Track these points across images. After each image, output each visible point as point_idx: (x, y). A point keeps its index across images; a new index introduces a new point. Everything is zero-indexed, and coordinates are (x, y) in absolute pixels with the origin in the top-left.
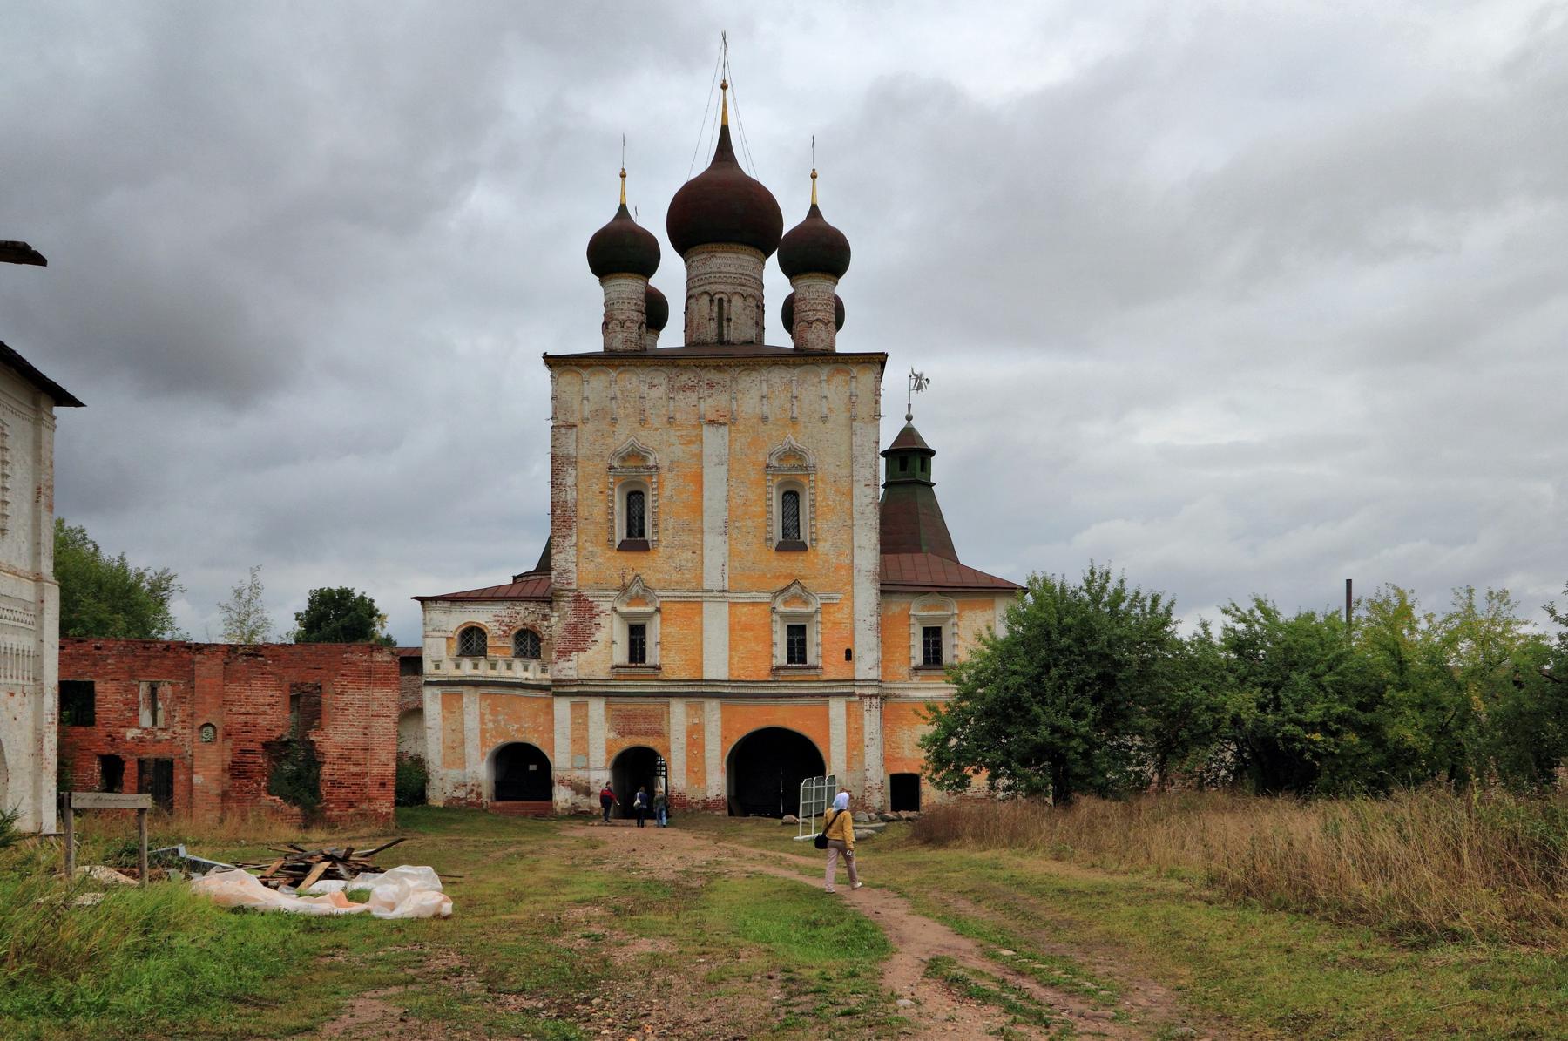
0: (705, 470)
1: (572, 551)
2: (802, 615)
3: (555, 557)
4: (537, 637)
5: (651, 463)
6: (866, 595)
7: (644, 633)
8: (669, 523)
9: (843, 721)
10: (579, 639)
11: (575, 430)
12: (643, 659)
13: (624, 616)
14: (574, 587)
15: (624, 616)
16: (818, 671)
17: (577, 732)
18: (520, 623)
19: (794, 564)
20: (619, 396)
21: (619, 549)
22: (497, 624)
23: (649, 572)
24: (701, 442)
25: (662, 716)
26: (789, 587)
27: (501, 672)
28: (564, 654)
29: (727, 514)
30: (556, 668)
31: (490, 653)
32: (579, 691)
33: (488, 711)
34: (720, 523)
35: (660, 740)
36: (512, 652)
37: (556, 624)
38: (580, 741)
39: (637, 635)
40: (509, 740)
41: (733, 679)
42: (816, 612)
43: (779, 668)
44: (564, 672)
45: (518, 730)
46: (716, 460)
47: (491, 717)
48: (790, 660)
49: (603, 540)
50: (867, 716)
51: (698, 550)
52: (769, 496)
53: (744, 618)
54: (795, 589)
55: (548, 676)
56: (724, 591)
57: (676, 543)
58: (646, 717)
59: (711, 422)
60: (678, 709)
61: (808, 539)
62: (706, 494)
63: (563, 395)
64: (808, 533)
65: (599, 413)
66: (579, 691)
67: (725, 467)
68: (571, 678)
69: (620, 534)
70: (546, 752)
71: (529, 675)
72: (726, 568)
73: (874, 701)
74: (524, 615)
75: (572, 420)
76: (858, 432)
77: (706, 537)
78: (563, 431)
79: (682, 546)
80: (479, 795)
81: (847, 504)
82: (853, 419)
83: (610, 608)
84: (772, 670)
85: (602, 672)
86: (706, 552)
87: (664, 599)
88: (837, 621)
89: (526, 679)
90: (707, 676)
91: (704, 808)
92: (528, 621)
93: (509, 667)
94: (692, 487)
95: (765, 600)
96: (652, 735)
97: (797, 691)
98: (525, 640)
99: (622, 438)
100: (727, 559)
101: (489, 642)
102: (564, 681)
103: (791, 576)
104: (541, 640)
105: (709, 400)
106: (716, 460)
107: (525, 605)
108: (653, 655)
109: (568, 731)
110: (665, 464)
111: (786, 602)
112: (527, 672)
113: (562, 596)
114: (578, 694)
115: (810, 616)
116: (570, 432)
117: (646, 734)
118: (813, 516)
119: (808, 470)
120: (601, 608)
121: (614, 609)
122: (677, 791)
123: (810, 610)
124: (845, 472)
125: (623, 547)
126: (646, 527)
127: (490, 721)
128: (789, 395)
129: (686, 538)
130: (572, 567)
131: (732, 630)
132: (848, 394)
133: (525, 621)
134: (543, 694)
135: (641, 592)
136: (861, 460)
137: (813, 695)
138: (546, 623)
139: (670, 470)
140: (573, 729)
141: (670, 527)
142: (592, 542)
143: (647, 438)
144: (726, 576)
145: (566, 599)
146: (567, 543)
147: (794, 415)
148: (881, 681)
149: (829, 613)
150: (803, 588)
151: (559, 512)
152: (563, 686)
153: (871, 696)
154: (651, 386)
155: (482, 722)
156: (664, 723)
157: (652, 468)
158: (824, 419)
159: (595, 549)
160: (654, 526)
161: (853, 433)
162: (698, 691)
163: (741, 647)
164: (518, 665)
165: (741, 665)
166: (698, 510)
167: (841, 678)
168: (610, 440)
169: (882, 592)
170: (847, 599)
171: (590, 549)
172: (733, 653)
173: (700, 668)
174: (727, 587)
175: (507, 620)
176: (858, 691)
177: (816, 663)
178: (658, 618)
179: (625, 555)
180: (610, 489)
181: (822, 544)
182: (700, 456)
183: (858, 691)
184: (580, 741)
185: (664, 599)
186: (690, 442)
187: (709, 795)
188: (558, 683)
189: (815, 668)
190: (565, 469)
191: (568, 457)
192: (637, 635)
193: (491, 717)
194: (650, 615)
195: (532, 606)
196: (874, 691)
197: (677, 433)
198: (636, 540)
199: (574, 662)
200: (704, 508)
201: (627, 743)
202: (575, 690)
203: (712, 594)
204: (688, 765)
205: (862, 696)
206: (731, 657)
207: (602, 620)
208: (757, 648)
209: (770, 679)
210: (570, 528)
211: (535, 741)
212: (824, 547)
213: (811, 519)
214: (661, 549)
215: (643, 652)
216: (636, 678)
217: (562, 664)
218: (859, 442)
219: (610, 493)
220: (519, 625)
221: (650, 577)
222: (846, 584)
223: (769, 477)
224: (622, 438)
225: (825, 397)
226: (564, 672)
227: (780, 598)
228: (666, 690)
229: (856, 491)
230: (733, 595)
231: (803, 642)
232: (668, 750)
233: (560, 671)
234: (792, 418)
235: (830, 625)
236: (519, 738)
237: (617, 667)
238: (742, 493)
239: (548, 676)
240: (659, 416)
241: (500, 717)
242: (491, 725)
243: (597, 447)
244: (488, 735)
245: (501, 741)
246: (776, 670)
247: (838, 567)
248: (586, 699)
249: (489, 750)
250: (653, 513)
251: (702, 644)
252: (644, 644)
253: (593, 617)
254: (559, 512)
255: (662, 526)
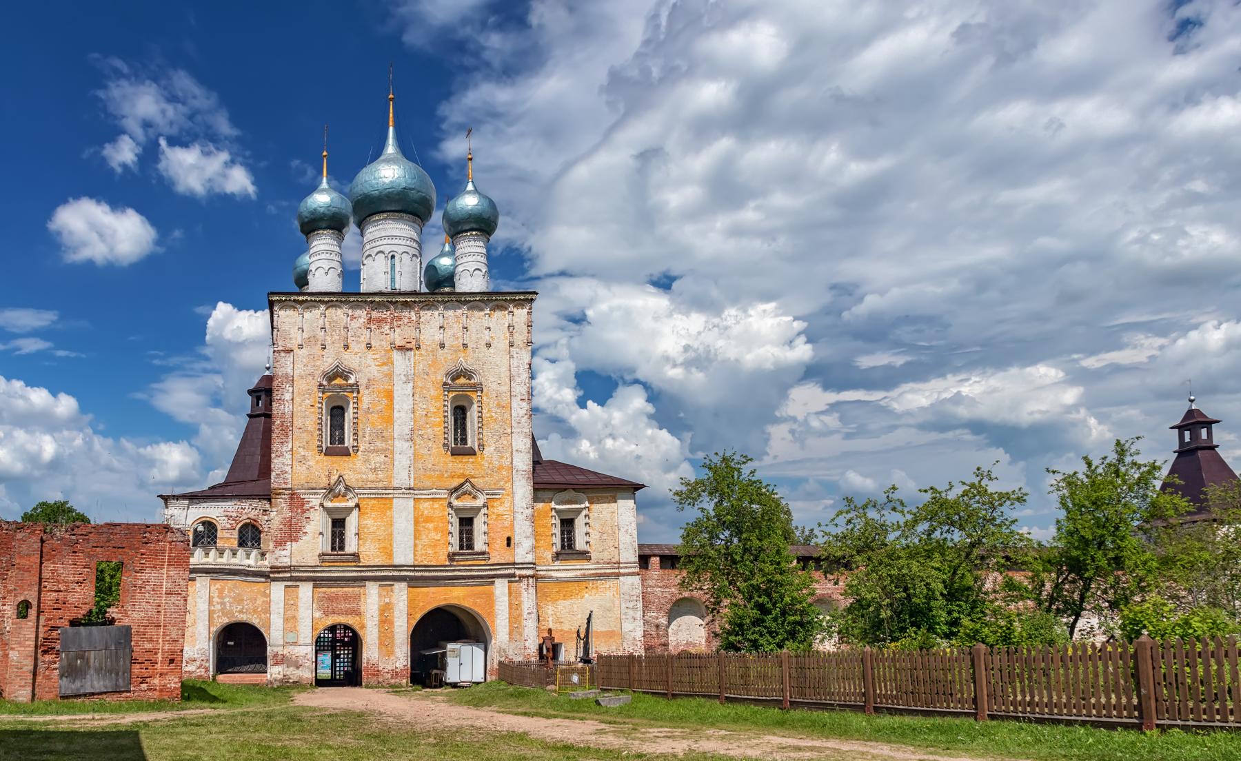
0: (395, 388)
1: (288, 456)
2: (472, 509)
3: (275, 461)
4: (257, 529)
5: (351, 381)
6: (522, 489)
7: (344, 526)
8: (367, 431)
9: (506, 598)
10: (292, 531)
11: (292, 354)
12: (342, 548)
13: (329, 511)
14: (289, 486)
15: (329, 511)
16: (486, 556)
17: (289, 612)
18: (245, 517)
19: (465, 466)
20: (327, 326)
21: (325, 455)
22: (226, 519)
23: (350, 473)
24: (393, 364)
25: (357, 598)
26: (462, 485)
27: (226, 560)
28: (280, 544)
29: (412, 423)
30: (274, 556)
31: (220, 543)
32: (290, 575)
33: (216, 594)
34: (407, 431)
35: (358, 618)
36: (236, 542)
37: (274, 518)
38: (290, 620)
39: (338, 525)
40: (233, 620)
41: (416, 563)
42: (484, 506)
43: (454, 554)
44: (281, 560)
45: (241, 612)
46: (404, 379)
47: (219, 601)
48: (461, 547)
49: (315, 447)
50: (525, 594)
51: (388, 453)
52: (446, 408)
53: (426, 512)
54: (467, 487)
55: (266, 563)
56: (410, 489)
57: (372, 448)
58: (346, 598)
59: (402, 349)
60: (372, 589)
61: (476, 444)
62: (396, 407)
63: (283, 325)
64: (476, 440)
65: (312, 340)
66: (290, 575)
67: (411, 385)
68: (285, 565)
69: (326, 443)
70: (262, 630)
71: (251, 562)
72: (412, 468)
73: (531, 580)
74: (249, 510)
75: (289, 346)
76: (515, 356)
77: (396, 442)
78: (283, 354)
79: (377, 451)
80: (207, 670)
81: (507, 416)
82: (511, 345)
83: (318, 504)
84: (449, 556)
85: (313, 560)
86: (397, 456)
87: (362, 496)
88: (500, 513)
89: (249, 566)
90: (397, 561)
91: (392, 678)
92: (251, 516)
93: (234, 554)
94: (385, 401)
95: (443, 496)
96: (351, 613)
97: (469, 573)
98: (247, 532)
99: (328, 362)
100: (412, 462)
101: (219, 534)
102: (280, 567)
103: (463, 475)
104: (260, 532)
105: (398, 330)
106: (404, 379)
107: (249, 502)
108: (351, 546)
109: (282, 611)
110: (363, 382)
111: (458, 498)
112: (250, 560)
113: (280, 494)
114: (291, 579)
115: (478, 509)
116: (288, 355)
117: (347, 612)
118: (480, 425)
119: (478, 388)
120: (311, 504)
121: (322, 505)
122: (371, 662)
123: (479, 502)
124: (505, 388)
125: (329, 453)
126: (346, 436)
127: (218, 603)
128: (461, 325)
129: (380, 445)
130: (288, 469)
131: (416, 522)
132: (507, 325)
133: (249, 516)
134: (263, 580)
135: (343, 490)
136: (518, 380)
137: (482, 577)
138: (266, 518)
139: (367, 387)
140: (286, 610)
141: (367, 435)
142: (304, 448)
143: (349, 360)
144: (412, 476)
145: (283, 496)
146: (284, 449)
147: (465, 342)
148: (534, 564)
149: (493, 507)
150: (473, 486)
151: (278, 422)
152: (279, 572)
153: (528, 577)
154: (353, 318)
155: (210, 602)
156: (361, 603)
157: (353, 385)
158: (489, 345)
159: (307, 454)
160: (355, 434)
161: (511, 357)
162: (388, 576)
163: (424, 537)
164: (241, 552)
165: (423, 552)
166: (390, 420)
167: (503, 561)
168: (318, 363)
169: (535, 490)
170: (508, 495)
171: (303, 454)
172: (417, 542)
173: (390, 555)
174: (412, 486)
175: (234, 514)
176: (518, 572)
177: (483, 550)
178: (355, 512)
179: (329, 458)
180: (319, 403)
181: (487, 449)
182: (390, 376)
183: (518, 572)
184: (290, 620)
185: (362, 496)
186: (384, 364)
187: (398, 665)
188: (276, 570)
189: (483, 553)
190: (284, 386)
191: (286, 376)
192: (338, 525)
193: (219, 601)
194: (350, 510)
195: (255, 503)
196: (530, 572)
197: (374, 357)
198: (336, 447)
199: (289, 550)
200: (395, 419)
201: (332, 620)
202: (288, 575)
203: (400, 491)
204: (379, 638)
205: (521, 577)
206: (415, 545)
207: (311, 514)
208: (436, 538)
209: (447, 563)
210: (287, 436)
211: (255, 621)
212: (489, 450)
213: (479, 428)
214: (359, 453)
215: (342, 541)
216: (338, 564)
217: (278, 552)
218: (516, 365)
219: (320, 406)
220: (244, 520)
221: (351, 478)
222: (506, 482)
223: (446, 393)
224: (330, 361)
225: (489, 328)
226: (281, 560)
227: (455, 495)
228: (363, 574)
229: (514, 405)
230: (416, 492)
231: (470, 532)
232: (363, 627)
233: (277, 559)
234: (463, 344)
235: (494, 517)
236: (243, 618)
237: (324, 555)
238: (424, 406)
239: (266, 563)
240: (358, 342)
241: (227, 600)
242: (219, 607)
243: (309, 368)
244: (215, 616)
245: (226, 621)
246: (452, 557)
247: (501, 468)
248: (298, 583)
249: (214, 629)
250: (354, 423)
251: (392, 534)
252: (344, 534)
253: (303, 512)
254: (278, 422)
255: (360, 433)
